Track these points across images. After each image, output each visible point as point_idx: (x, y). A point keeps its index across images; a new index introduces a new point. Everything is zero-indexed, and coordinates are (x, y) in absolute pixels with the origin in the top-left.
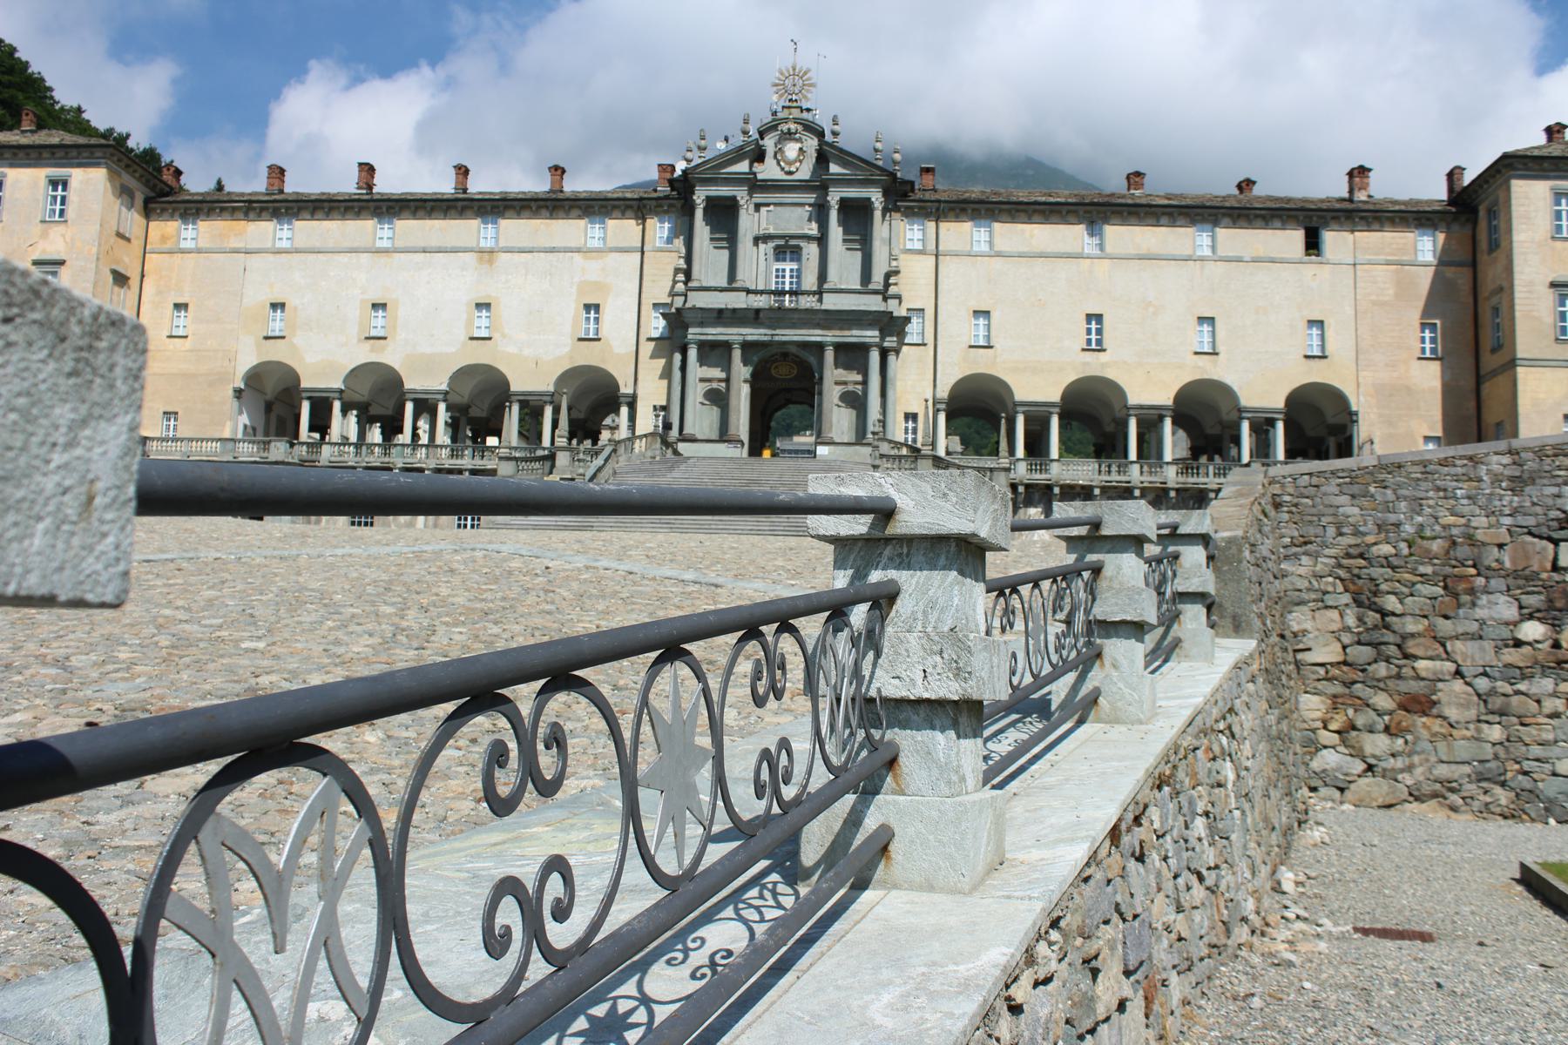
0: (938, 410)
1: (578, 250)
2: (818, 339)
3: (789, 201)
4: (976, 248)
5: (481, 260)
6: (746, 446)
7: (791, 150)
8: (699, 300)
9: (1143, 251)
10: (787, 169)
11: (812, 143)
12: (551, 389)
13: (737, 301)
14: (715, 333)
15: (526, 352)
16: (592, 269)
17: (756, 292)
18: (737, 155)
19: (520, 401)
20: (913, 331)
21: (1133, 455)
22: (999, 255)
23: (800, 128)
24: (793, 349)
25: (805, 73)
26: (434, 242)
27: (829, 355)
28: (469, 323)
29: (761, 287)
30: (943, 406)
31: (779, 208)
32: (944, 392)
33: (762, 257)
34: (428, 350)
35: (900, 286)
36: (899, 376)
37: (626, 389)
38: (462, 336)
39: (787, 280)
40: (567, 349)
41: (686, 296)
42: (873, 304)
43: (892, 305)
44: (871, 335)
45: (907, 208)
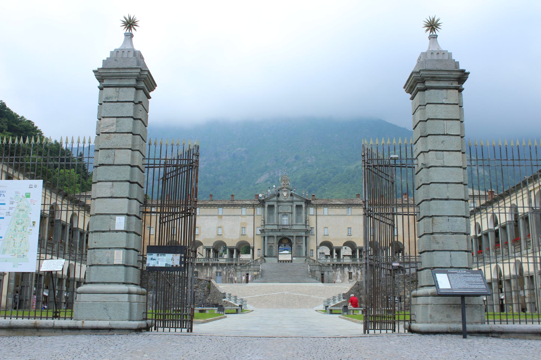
1: (240, 215)
2: (292, 235)
5: (219, 218)
7: (285, 194)
9: (359, 214)
11: (290, 192)
12: (235, 246)
14: (271, 234)
15: (230, 238)
16: (243, 220)
18: (274, 195)
19: (229, 248)
21: (358, 257)
22: (329, 215)
24: (287, 237)
26: (208, 214)
27: (295, 238)
28: (217, 231)
32: (318, 245)
34: (208, 237)
37: (252, 246)
38: (215, 234)
40: (238, 237)
42: (304, 227)
44: (303, 234)
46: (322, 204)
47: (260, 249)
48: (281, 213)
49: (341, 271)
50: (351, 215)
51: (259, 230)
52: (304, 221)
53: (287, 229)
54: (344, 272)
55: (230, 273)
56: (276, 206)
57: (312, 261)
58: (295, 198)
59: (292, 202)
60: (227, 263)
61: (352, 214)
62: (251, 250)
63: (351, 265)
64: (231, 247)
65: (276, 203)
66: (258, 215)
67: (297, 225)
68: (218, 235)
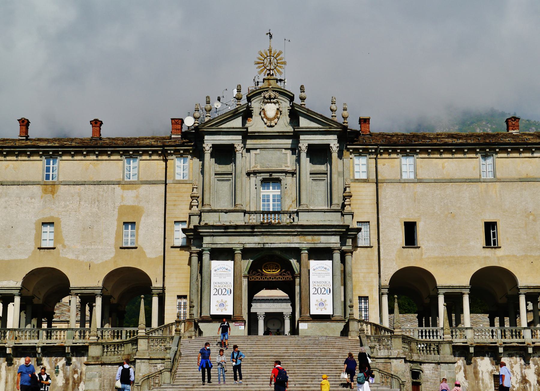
0: (383, 294)
1: (118, 183)
3: (271, 146)
4: (405, 176)
5: (45, 191)
6: (247, 324)
7: (271, 109)
8: (210, 219)
9: (524, 176)
10: (268, 124)
11: (285, 105)
12: (100, 285)
13: (238, 219)
14: (222, 242)
15: (81, 258)
17: (250, 213)
18: (234, 115)
20: (363, 239)
22: (420, 181)
23: (277, 94)
25: (278, 55)
28: (38, 237)
29: (253, 209)
30: (386, 291)
31: (264, 152)
32: (386, 282)
33: (253, 187)
35: (354, 206)
36: (354, 270)
37: (156, 284)
38: (31, 246)
39: (271, 203)
40: (112, 255)
41: (200, 216)
42: (335, 219)
43: (348, 220)
44: (334, 241)
45: (354, 149)
46: (395, 144)
47: (185, 297)
48: (255, 173)
49: (465, 371)
50: (496, 180)
51: (184, 231)
52: (337, 200)
53: (278, 226)
54: (476, 373)
55: (80, 379)
56: (239, 147)
57: (368, 329)
58: (304, 123)
59: (295, 136)
60: (69, 343)
61: (498, 175)
62: (155, 300)
63: (501, 350)
64: (85, 289)
65: (240, 137)
66: (179, 182)
67: (312, 211)
68: (40, 248)
